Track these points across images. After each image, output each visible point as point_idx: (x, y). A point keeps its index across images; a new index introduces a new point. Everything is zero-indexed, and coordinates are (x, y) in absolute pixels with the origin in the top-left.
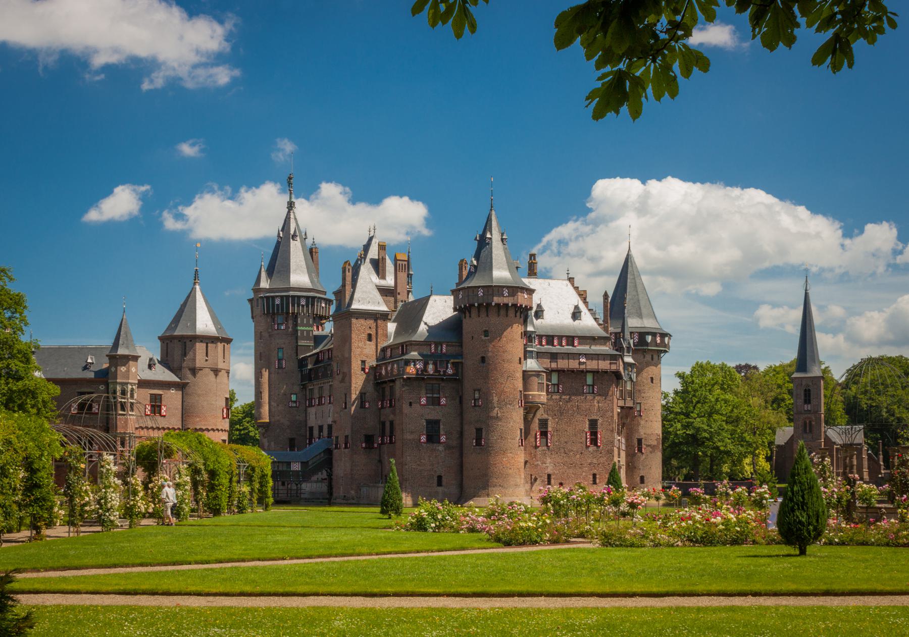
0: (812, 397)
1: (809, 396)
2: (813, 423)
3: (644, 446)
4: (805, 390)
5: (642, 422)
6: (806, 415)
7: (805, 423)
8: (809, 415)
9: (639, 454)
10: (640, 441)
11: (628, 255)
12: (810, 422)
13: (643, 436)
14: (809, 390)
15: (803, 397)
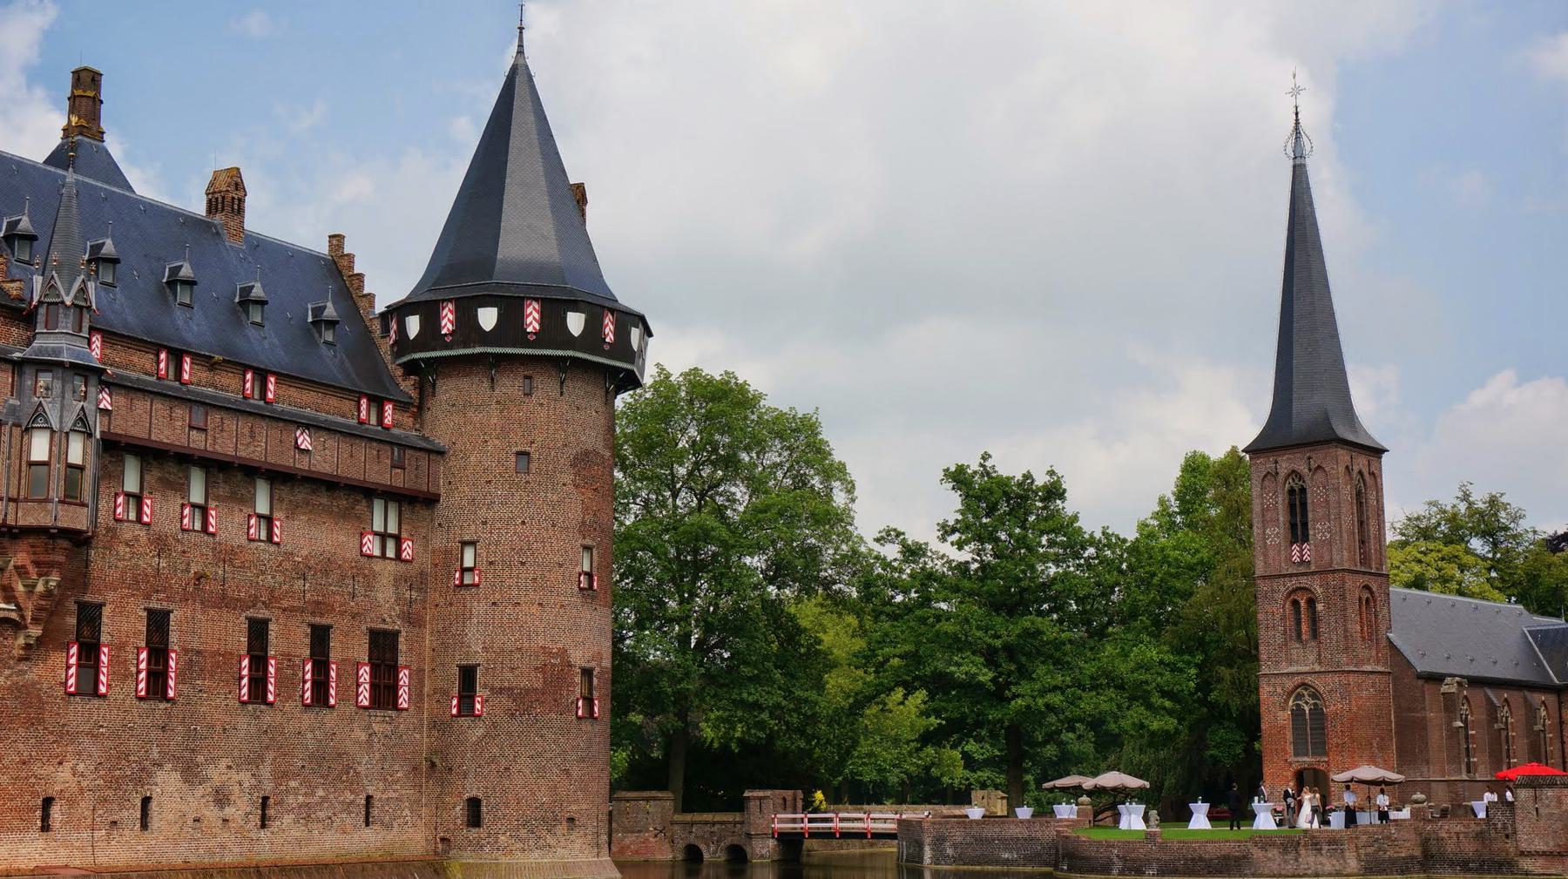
0: (1310, 516)
1: (1304, 505)
2: (1320, 607)
3: (481, 693)
4: (1292, 492)
5: (479, 608)
6: (1294, 581)
7: (1295, 603)
8: (1304, 581)
9: (464, 722)
10: (468, 675)
11: (514, 70)
12: (1311, 602)
13: (479, 659)
14: (1303, 490)
15: (1283, 517)
